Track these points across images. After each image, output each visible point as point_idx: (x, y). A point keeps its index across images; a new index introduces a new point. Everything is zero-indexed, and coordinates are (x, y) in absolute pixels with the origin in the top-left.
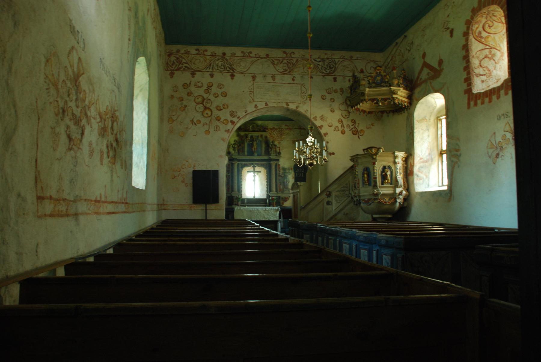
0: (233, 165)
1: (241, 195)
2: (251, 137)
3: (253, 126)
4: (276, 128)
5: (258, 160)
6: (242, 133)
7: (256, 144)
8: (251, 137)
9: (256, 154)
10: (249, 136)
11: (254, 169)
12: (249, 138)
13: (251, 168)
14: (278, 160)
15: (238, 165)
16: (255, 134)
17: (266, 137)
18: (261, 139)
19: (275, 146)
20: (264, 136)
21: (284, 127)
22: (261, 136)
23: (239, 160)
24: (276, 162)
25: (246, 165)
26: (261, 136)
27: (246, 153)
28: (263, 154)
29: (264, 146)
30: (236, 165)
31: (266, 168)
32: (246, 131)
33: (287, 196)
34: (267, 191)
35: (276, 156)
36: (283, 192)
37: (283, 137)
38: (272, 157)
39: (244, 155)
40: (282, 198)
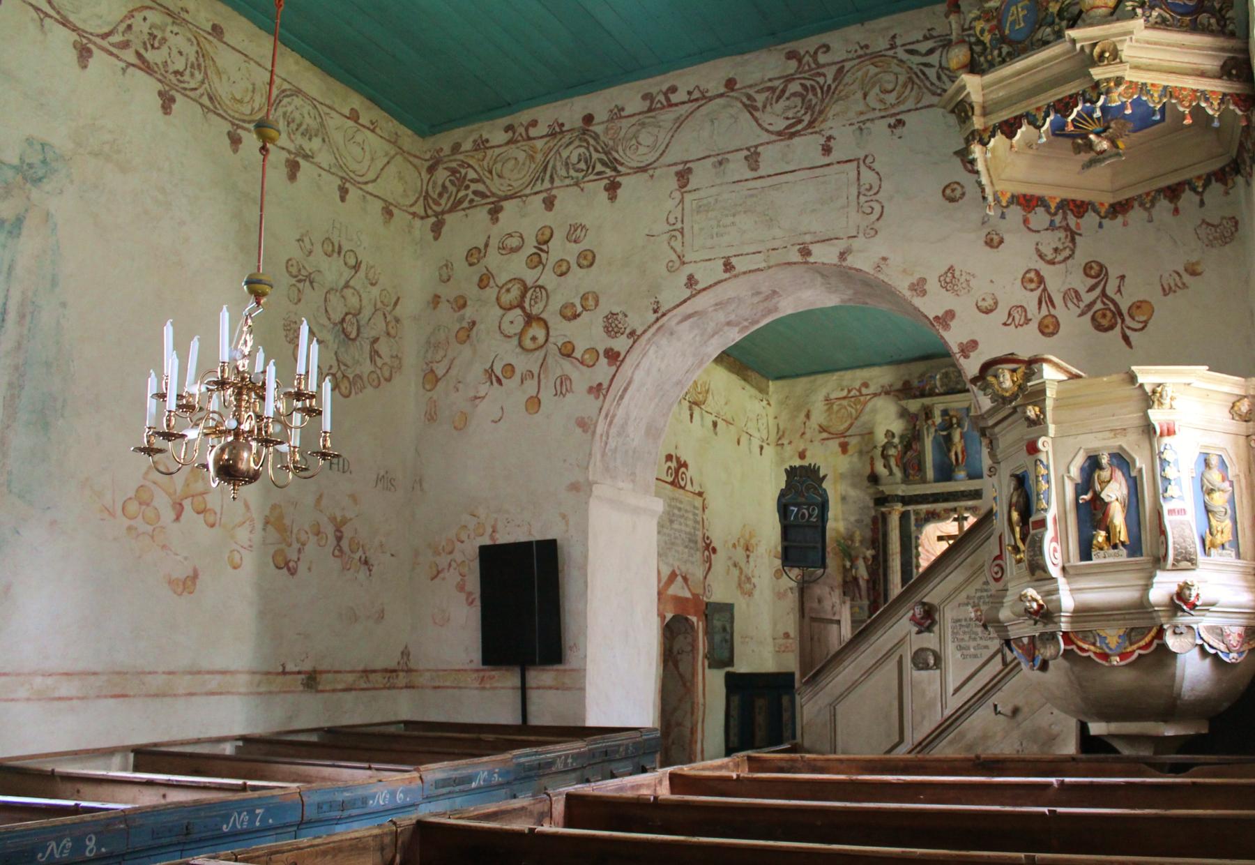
0: (884, 518)
2: (945, 413)
3: (946, 375)
6: (914, 405)
7: (962, 436)
9: (961, 474)
12: (938, 420)
15: (904, 517)
23: (906, 500)
25: (933, 516)
27: (930, 473)
30: (894, 520)
32: (923, 395)
39: (924, 481)
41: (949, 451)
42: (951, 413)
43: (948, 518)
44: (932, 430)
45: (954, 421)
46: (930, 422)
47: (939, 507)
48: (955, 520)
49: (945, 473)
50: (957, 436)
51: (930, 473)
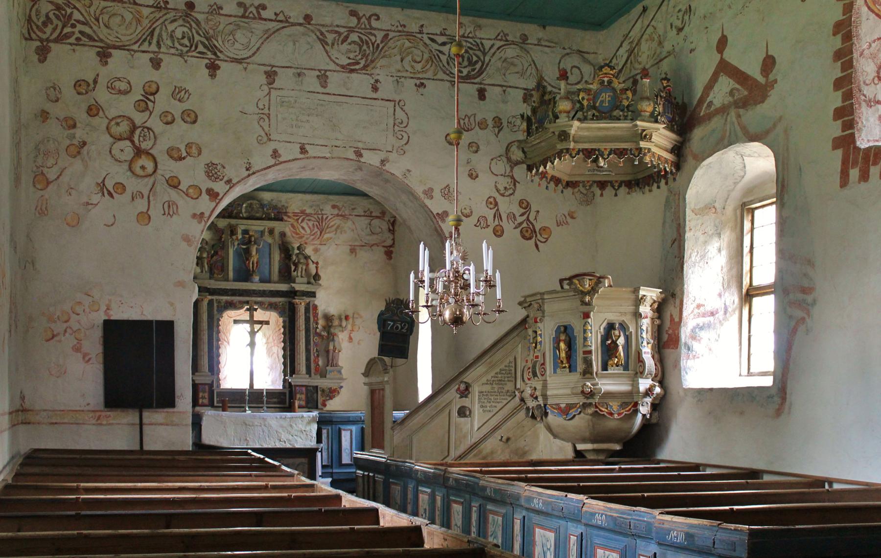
1: (219, 380)
3: (250, 205)
4: (308, 211)
5: (263, 293)
8: (246, 232)
10: (240, 231)
11: (252, 316)
12: (240, 237)
13: (242, 314)
14: (313, 295)
16: (256, 226)
17: (283, 235)
18: (270, 240)
19: (307, 258)
20: (277, 233)
21: (328, 210)
22: (271, 232)
24: (308, 300)
26: (271, 232)
27: (231, 275)
28: (275, 275)
29: (277, 257)
31: (281, 314)
32: (230, 216)
33: (334, 386)
34: (285, 372)
35: (309, 283)
36: (323, 375)
37: (326, 236)
38: (298, 287)
39: (227, 280)
40: (323, 391)
41: (247, 259)
42: (251, 233)
43: (242, 308)
44: (236, 243)
45: (253, 239)
46: (234, 237)
47: (236, 299)
48: (247, 310)
49: (244, 275)
50: (254, 253)
51: (231, 275)
